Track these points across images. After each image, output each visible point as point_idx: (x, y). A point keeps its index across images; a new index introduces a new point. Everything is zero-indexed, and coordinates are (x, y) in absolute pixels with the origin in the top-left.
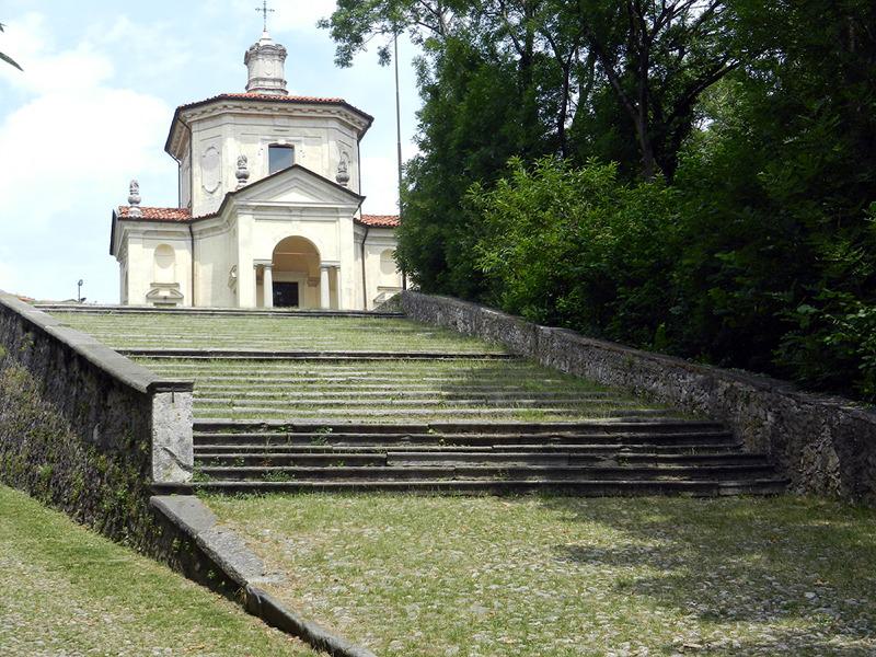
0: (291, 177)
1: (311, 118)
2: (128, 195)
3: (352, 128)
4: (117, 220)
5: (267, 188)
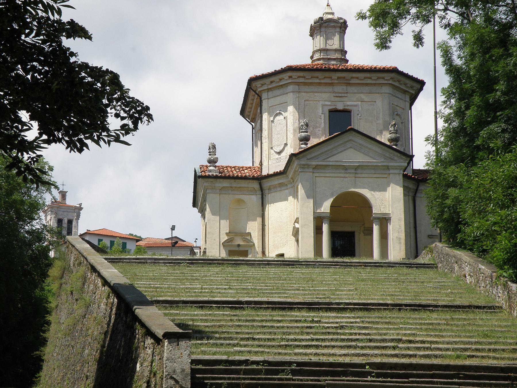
1: (367, 84)
3: (405, 92)
4: (197, 177)
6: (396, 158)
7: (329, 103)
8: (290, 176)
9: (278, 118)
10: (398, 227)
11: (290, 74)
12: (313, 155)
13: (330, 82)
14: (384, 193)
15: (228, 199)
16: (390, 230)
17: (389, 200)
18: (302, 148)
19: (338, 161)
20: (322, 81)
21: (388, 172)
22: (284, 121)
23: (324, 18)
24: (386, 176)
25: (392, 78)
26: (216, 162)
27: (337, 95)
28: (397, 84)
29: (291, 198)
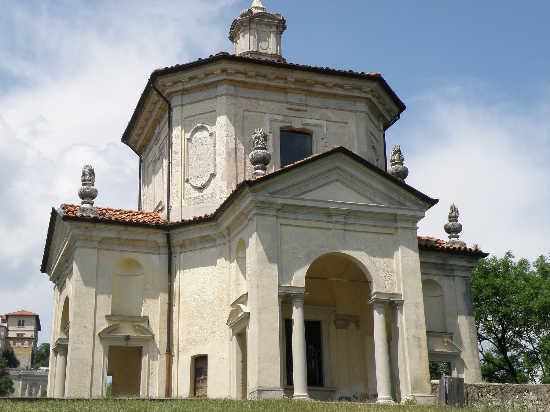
0: (331, 167)
1: (335, 96)
2: (78, 186)
5: (299, 179)
6: (408, 203)
7: (280, 118)
8: (225, 224)
9: (198, 135)
10: (415, 318)
11: (224, 65)
12: (278, 187)
13: (283, 85)
14: (389, 260)
15: (112, 259)
16: (401, 322)
17: (395, 272)
18: (258, 175)
19: (318, 201)
20: (272, 83)
21: (394, 225)
22: (211, 140)
23: (254, 13)
24: (391, 231)
25: (371, 91)
26: (93, 197)
27: (293, 107)
28: (375, 101)
29: (221, 262)
